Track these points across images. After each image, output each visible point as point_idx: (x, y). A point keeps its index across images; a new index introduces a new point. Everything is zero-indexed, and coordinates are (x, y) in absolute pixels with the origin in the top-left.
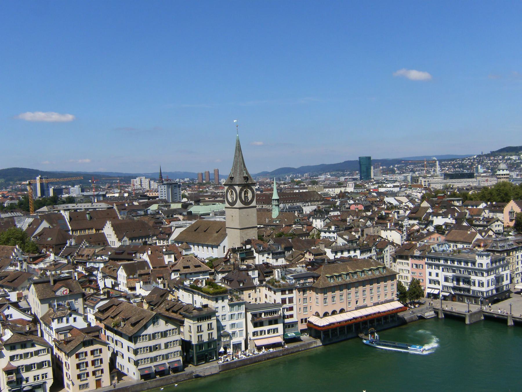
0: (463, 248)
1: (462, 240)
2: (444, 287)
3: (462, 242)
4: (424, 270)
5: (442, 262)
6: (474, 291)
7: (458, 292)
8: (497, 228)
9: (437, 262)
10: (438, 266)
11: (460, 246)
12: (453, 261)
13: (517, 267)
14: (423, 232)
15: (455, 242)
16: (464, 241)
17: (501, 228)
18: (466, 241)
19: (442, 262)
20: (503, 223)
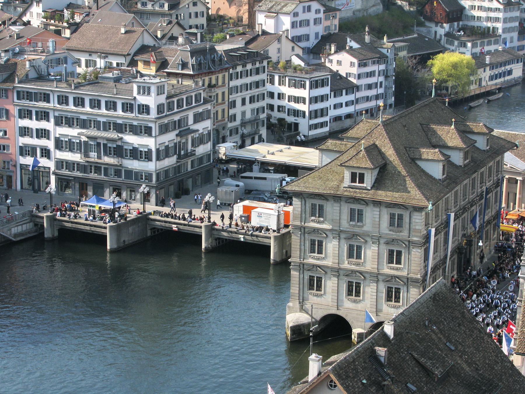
0: (109, 67)
1: (107, 49)
2: (60, 164)
3: (105, 55)
4: (10, 123)
5: (53, 104)
6: (129, 173)
7: (93, 175)
8: (193, 21)
9: (42, 104)
10: (44, 115)
11: (101, 63)
12: (79, 102)
13: (232, 112)
14: (13, 28)
15: (91, 53)
16: (112, 50)
17: (203, 21)
18: (116, 50)
19: (53, 104)
20: (208, 9)
